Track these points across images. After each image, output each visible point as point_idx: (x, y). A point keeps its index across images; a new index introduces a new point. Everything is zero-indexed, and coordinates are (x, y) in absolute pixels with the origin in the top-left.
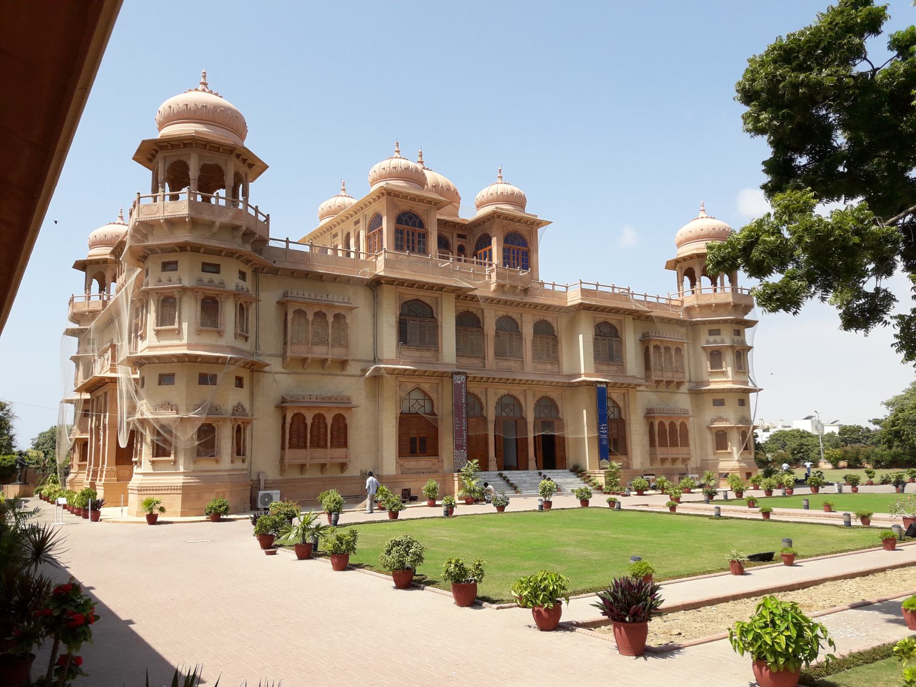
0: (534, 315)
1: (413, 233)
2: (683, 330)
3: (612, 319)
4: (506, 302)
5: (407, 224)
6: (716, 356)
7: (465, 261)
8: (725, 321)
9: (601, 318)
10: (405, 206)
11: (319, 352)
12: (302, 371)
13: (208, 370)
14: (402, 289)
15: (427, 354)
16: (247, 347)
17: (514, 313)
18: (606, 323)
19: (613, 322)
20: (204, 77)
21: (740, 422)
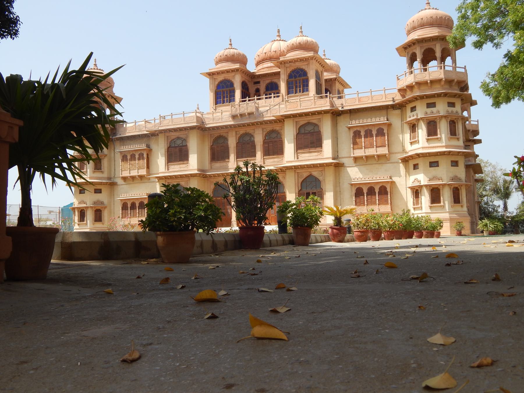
0: (263, 129)
1: (227, 92)
2: (398, 112)
3: (313, 119)
4: (239, 126)
5: (223, 87)
6: (413, 127)
7: (249, 100)
8: (416, 99)
9: (303, 121)
10: (220, 78)
11: (134, 173)
12: (132, 182)
13: (98, 187)
14: (167, 134)
15: (184, 166)
16: (105, 175)
17: (249, 130)
18: (309, 124)
19: (314, 121)
20: (95, 61)
21: (452, 180)
